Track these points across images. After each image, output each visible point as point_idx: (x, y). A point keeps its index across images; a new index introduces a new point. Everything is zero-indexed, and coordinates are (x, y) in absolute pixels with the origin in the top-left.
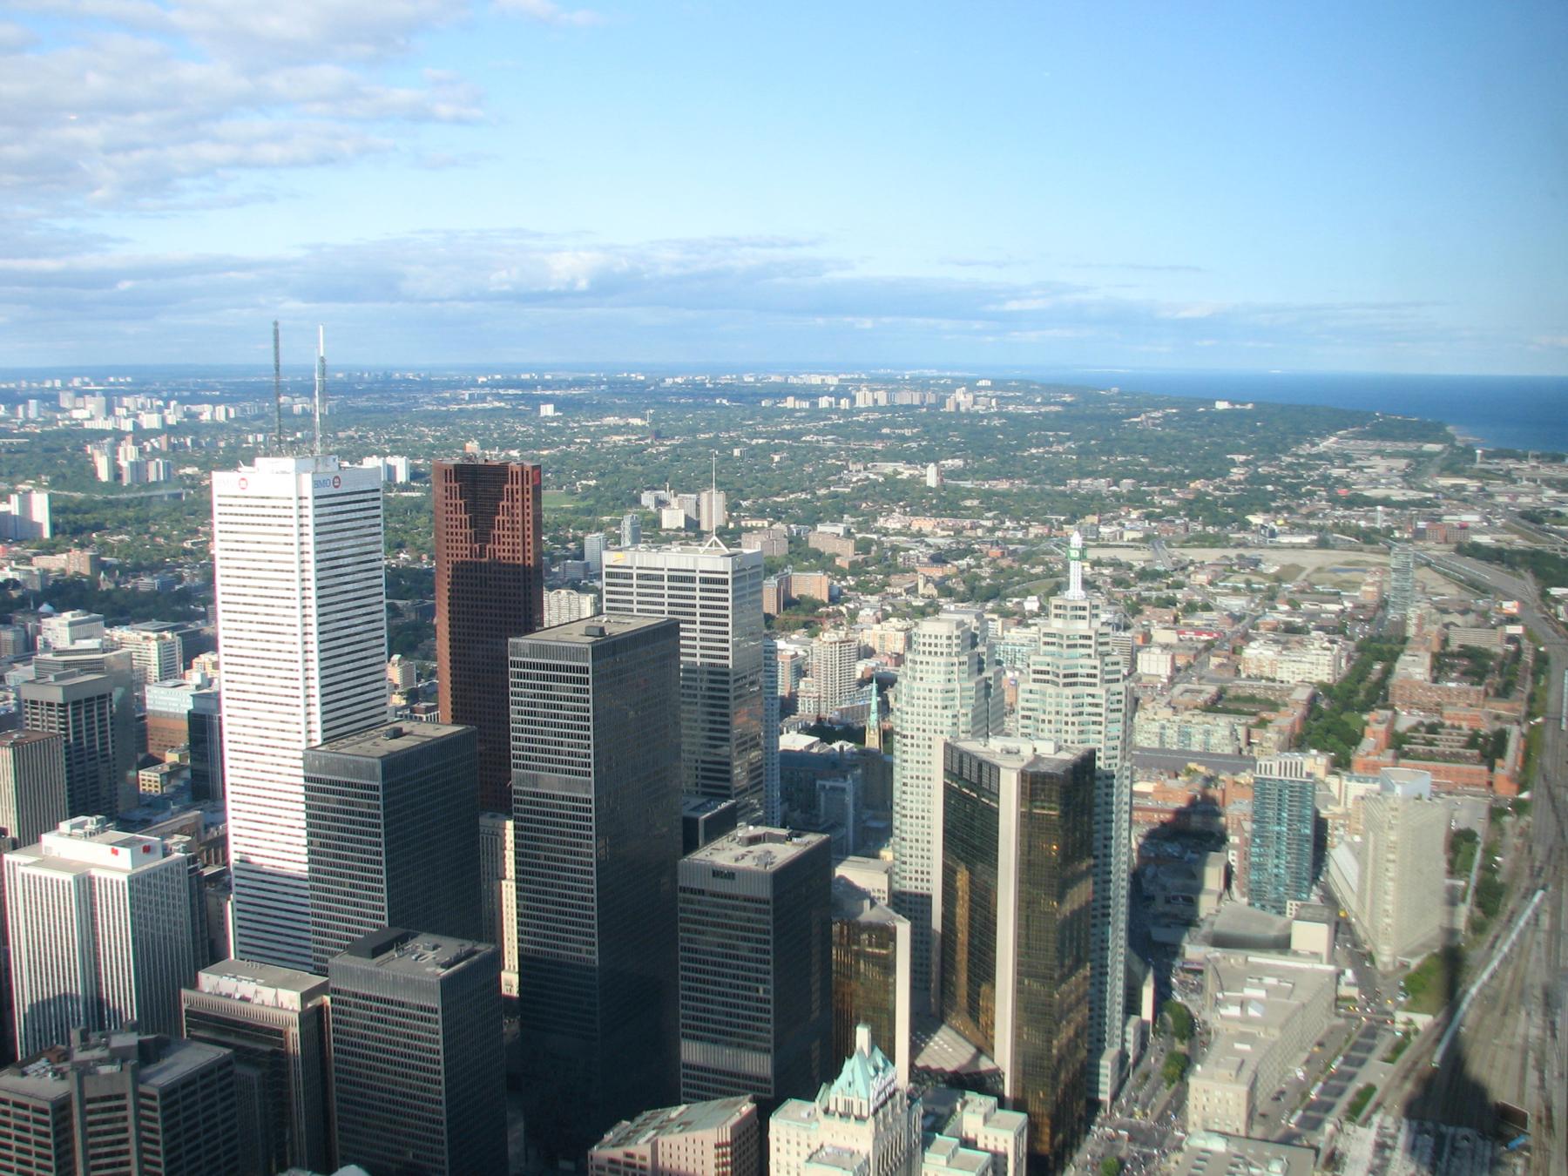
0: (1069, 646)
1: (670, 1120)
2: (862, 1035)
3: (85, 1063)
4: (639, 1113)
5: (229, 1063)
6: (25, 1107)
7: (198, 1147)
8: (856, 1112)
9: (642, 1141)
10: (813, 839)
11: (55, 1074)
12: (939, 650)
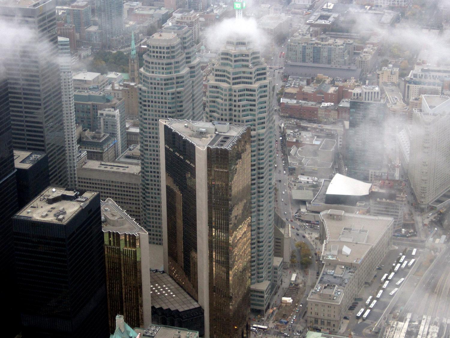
0: (235, 61)
2: (120, 320)
12: (162, 55)
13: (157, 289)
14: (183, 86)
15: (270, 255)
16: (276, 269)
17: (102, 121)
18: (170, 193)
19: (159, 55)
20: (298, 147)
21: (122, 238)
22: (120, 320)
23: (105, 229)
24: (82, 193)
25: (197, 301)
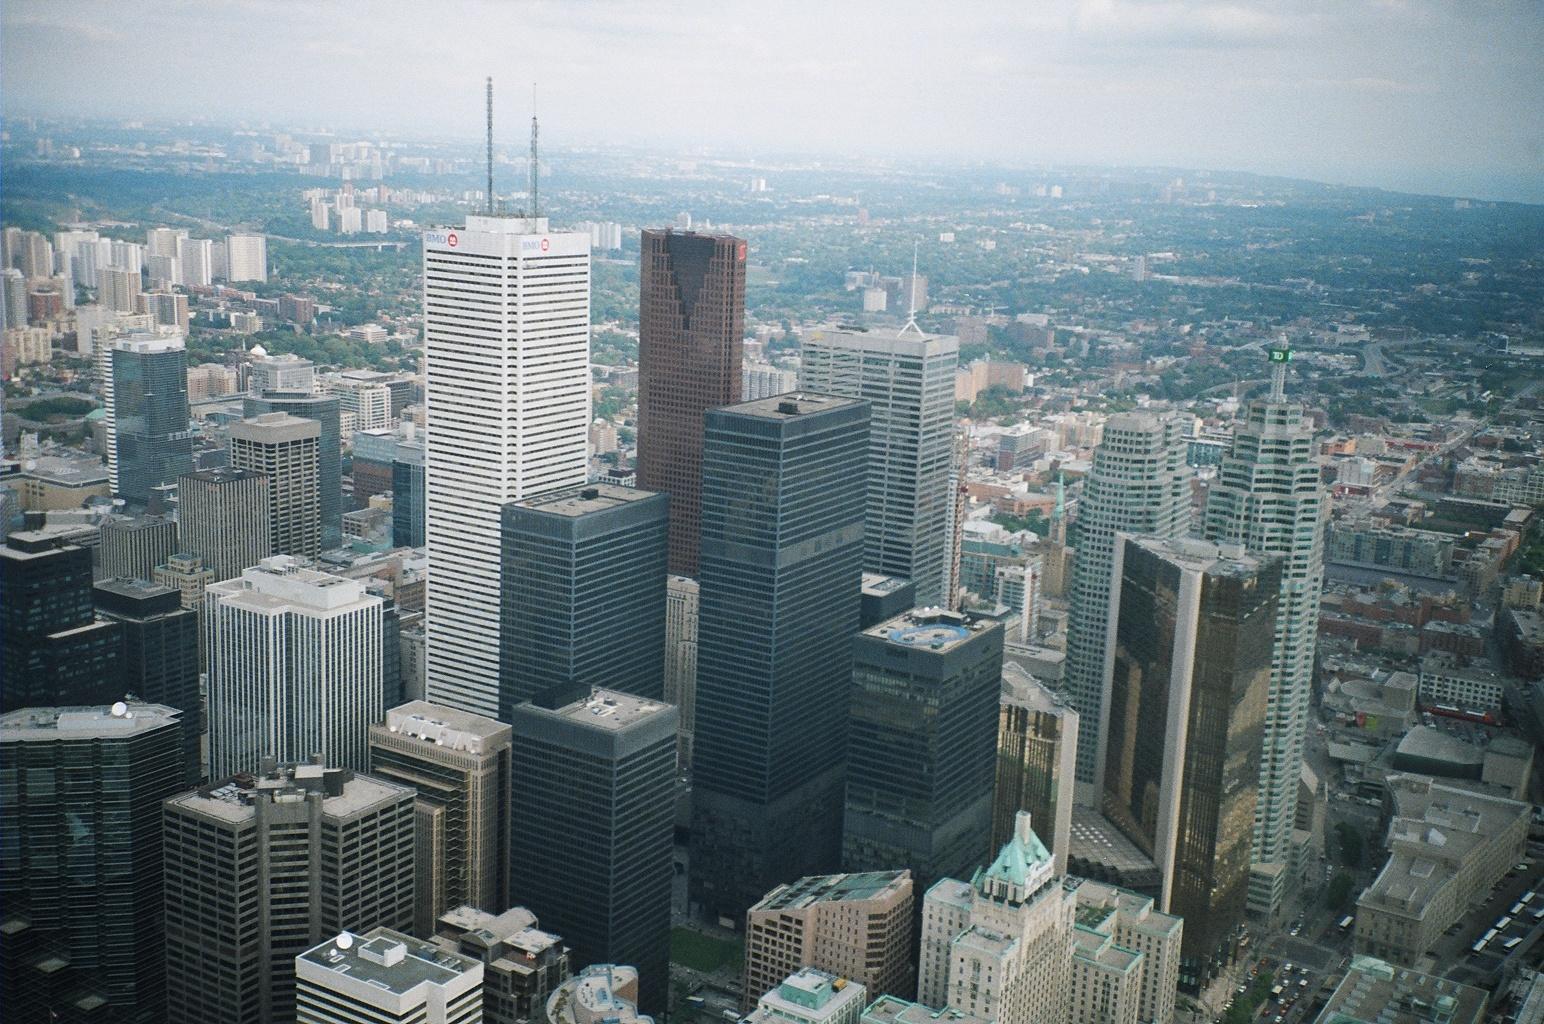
1: (828, 888)
2: (1023, 820)
3: (270, 792)
4: (798, 878)
5: (410, 800)
6: (211, 828)
7: (374, 878)
8: (1010, 897)
9: (799, 906)
10: (986, 625)
11: (243, 798)
12: (1128, 446)
13: (1079, 829)
14: (1158, 504)
15: (1288, 825)
16: (1296, 848)
17: (1001, 582)
18: (1121, 670)
19: (1121, 445)
20: (1342, 681)
21: (1031, 717)
22: (1023, 820)
23: (1005, 700)
24: (975, 618)
25: (1151, 858)
